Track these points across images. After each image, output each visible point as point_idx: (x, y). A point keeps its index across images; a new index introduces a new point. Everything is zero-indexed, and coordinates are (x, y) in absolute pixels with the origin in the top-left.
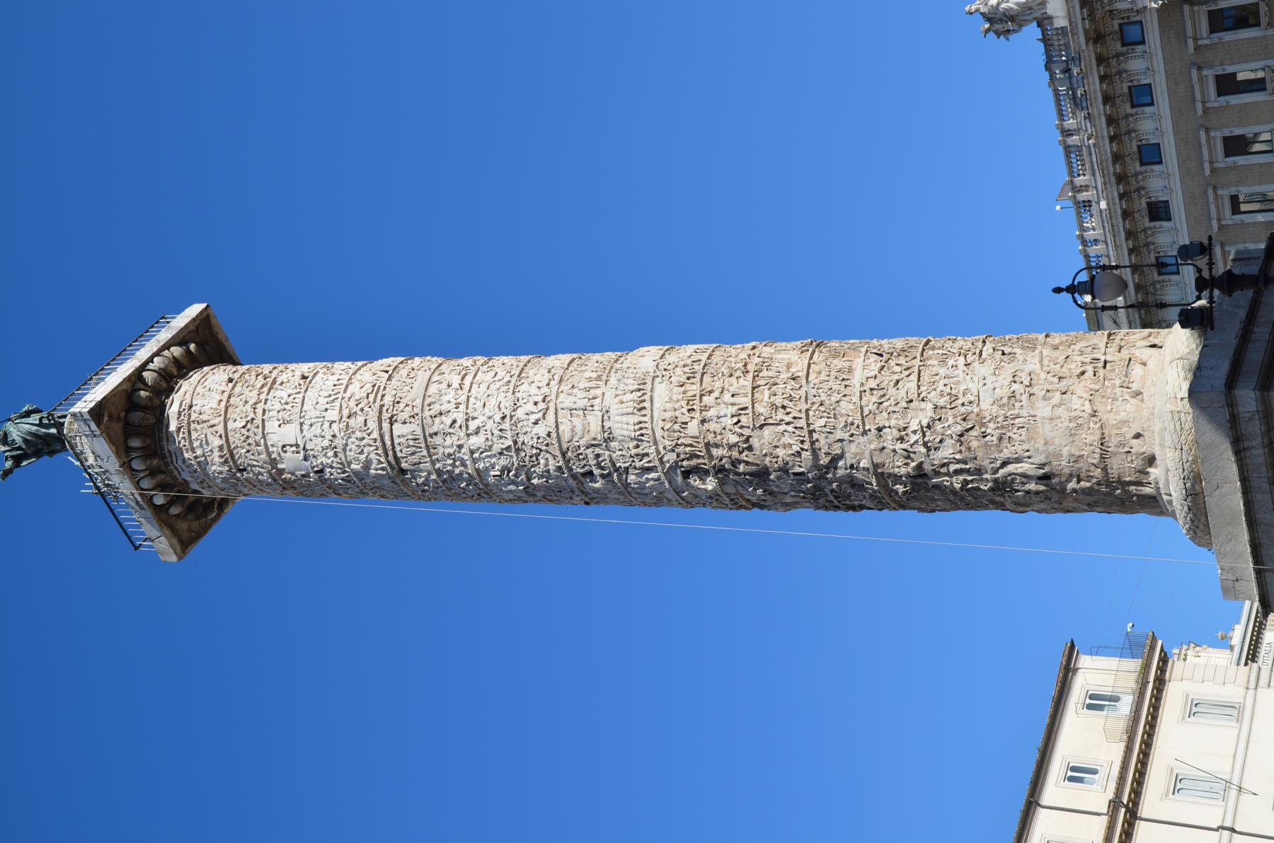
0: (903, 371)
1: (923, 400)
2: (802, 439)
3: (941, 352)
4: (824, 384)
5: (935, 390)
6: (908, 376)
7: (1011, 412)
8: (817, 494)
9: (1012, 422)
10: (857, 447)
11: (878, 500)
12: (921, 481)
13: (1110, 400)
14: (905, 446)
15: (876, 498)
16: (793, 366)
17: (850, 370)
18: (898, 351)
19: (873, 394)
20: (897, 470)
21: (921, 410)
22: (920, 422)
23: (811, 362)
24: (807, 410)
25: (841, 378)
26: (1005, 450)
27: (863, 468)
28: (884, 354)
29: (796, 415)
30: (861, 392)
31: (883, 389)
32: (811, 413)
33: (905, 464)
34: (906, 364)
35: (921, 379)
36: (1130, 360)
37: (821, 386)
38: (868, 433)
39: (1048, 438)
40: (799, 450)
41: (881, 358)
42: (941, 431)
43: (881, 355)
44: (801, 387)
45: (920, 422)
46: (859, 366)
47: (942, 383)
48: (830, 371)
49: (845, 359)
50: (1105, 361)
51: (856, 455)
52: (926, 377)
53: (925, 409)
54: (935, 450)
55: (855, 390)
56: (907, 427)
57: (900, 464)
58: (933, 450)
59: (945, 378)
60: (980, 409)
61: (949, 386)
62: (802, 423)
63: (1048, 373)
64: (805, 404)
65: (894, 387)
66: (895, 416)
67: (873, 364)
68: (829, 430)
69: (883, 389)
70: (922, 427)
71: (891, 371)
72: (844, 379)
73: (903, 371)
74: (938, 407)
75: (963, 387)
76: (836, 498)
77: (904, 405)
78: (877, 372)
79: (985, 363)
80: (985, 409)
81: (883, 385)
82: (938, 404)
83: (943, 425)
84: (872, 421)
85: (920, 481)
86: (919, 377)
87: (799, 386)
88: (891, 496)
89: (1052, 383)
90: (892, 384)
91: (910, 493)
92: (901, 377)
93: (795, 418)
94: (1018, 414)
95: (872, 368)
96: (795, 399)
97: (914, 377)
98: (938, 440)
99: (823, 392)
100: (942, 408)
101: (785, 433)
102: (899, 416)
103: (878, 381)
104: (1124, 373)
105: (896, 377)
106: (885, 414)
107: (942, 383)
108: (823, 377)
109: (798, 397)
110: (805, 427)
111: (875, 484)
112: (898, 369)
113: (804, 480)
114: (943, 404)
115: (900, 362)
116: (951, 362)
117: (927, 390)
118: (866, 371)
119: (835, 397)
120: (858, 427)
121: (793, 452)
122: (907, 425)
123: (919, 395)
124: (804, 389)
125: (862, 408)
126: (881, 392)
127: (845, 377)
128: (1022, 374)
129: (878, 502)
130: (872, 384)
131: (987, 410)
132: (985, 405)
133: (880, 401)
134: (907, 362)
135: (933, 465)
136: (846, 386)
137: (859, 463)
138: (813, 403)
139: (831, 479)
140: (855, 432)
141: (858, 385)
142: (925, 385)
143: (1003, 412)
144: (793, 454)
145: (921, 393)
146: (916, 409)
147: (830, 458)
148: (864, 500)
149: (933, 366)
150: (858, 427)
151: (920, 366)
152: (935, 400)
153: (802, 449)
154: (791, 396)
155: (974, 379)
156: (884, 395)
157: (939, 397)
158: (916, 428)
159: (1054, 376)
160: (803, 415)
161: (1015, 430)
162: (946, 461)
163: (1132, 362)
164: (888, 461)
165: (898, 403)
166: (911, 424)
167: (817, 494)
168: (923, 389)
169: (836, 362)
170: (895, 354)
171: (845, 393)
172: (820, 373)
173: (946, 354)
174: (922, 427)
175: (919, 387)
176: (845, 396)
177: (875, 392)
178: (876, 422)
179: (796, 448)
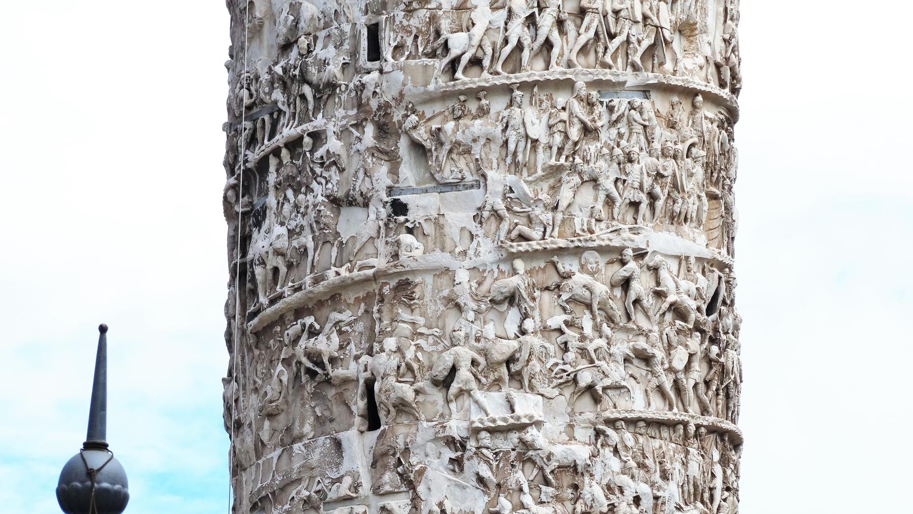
0: (672, 377)
1: (598, 433)
2: (486, 62)
3: (718, 483)
4: (642, 138)
5: (625, 470)
6: (660, 389)
8: (307, 90)
10: (463, 229)
11: (283, 270)
12: (354, 408)
14: (464, 373)
15: (290, 266)
16: (685, 43)
17: (676, 218)
18: (722, 360)
19: (613, 286)
20: (390, 343)
21: (571, 426)
22: (538, 424)
23: (700, 98)
24: (568, 85)
25: (657, 189)
27: (398, 243)
28: (714, 316)
29: (556, 51)
30: (621, 250)
31: (629, 318)
32: (561, 99)
33: (409, 368)
34: (692, 383)
35: (652, 431)
37: (638, 128)
38: (504, 267)
40: (454, 52)
41: (704, 307)
42: (512, 482)
43: (710, 310)
44: (635, 68)
45: (538, 424)
46: (689, 243)
47: (644, 489)
48: (675, 157)
49: (705, 199)
51: (438, 222)
52: (656, 443)
53: (572, 438)
54: (452, 461)
55: (627, 234)
56: (521, 382)
57: (410, 354)
58: (453, 455)
59: (656, 498)
62: (534, 71)
64: (590, 78)
65: (635, 350)
66: (552, 348)
67: (693, 287)
68: (512, 146)
69: (629, 318)
70: (522, 427)
71: (674, 339)
72: (653, 197)
73: (672, 377)
74: (578, 480)
76: (294, 145)
77: (585, 379)
78: (671, 298)
81: (640, 319)
82: (587, 479)
83: (526, 488)
84: (539, 279)
85: (360, 405)
86: (659, 424)
87: (637, 59)
88: (299, 312)
90: (642, 343)
91: (312, 374)
92: (659, 369)
93: (548, 45)
95: (684, 284)
96: (601, 50)
97: (657, 409)
98: (486, 472)
99: (620, 136)
100: (576, 487)
101: (503, 13)
102: (552, 361)
103: (649, 301)
105: (659, 354)
106: (557, 320)
107: (644, 489)
108: (661, 134)
109: (608, 59)
110: (523, 77)
111: (344, 272)
112: (679, 359)
113: (354, 54)
114: (586, 491)
115: (696, 365)
118: (674, 265)
119: (608, 173)
120: (522, 237)
121: (445, 34)
122: (526, 383)
124: (631, 79)
125: (578, 251)
126: (619, 313)
127: (659, 204)
129: (276, 270)
130: (641, 286)
133: (595, 307)
134: (695, 386)
135: (407, 450)
136: (635, 205)
137: (410, 231)
138: (591, 105)
139: (360, 139)
140: (505, 226)
141: (639, 241)
142: (637, 441)
144: (438, 34)
145: (616, 429)
146: (572, 414)
147: (428, 144)
148: (283, 231)
149: (685, 464)
150: (522, 237)
151: (685, 424)
152: (598, 470)
153: (453, 65)
154: (612, 36)
156: (610, 319)
157: (605, 482)
158: (519, 411)
160: (557, 72)
162: (421, 489)
164: (421, 321)
165: (592, 361)
166: (530, 396)
167: (307, 90)
168: (629, 437)
169: (699, 171)
170: (715, 349)
171: (619, 201)
172: (672, 125)
173: (712, 499)
174: (522, 427)
175: (632, 422)
176: (610, 201)
177: (618, 292)
178: (537, 294)
179: (458, 43)
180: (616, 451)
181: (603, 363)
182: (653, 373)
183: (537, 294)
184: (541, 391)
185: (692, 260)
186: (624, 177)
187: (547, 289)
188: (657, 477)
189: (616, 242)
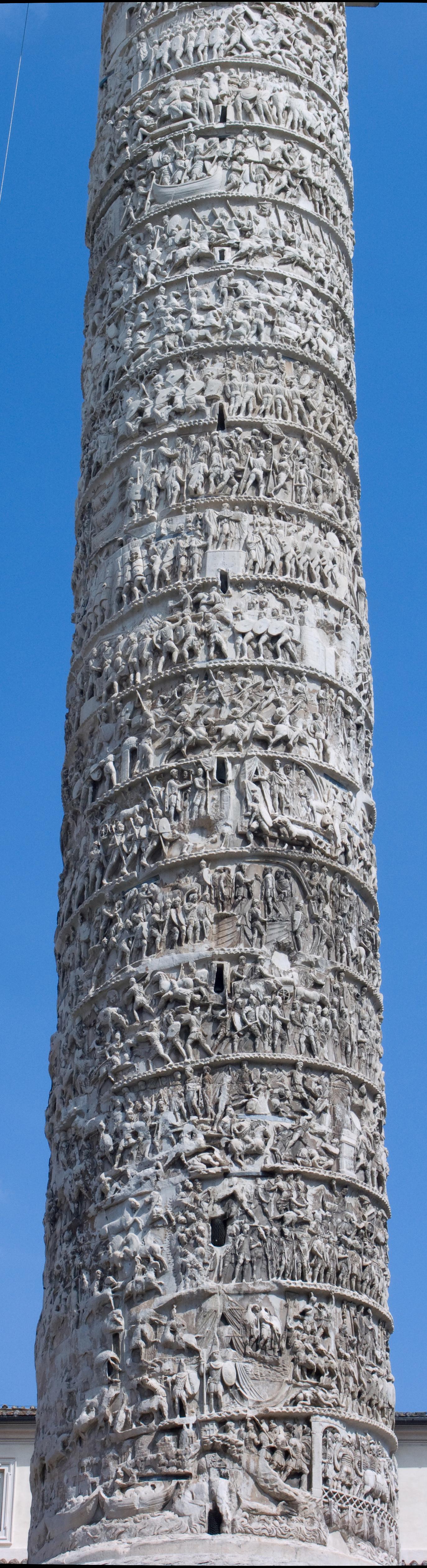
36: (187, 1476)
50: (180, 1427)
61: (132, 1141)
63: (154, 1325)
73: (169, 1045)
75: (131, 1169)
94: (83, 1291)
104: (150, 1471)
128: (151, 1274)
131: (94, 1230)
141: (140, 970)
143: (87, 1261)
151: (183, 1071)
154: (127, 855)
159: (144, 1337)
161: (64, 1295)
163: (174, 1482)
173: (216, 1109)
180: (123, 1109)
183: (86, 1032)
185: (192, 964)
187: (90, 1026)
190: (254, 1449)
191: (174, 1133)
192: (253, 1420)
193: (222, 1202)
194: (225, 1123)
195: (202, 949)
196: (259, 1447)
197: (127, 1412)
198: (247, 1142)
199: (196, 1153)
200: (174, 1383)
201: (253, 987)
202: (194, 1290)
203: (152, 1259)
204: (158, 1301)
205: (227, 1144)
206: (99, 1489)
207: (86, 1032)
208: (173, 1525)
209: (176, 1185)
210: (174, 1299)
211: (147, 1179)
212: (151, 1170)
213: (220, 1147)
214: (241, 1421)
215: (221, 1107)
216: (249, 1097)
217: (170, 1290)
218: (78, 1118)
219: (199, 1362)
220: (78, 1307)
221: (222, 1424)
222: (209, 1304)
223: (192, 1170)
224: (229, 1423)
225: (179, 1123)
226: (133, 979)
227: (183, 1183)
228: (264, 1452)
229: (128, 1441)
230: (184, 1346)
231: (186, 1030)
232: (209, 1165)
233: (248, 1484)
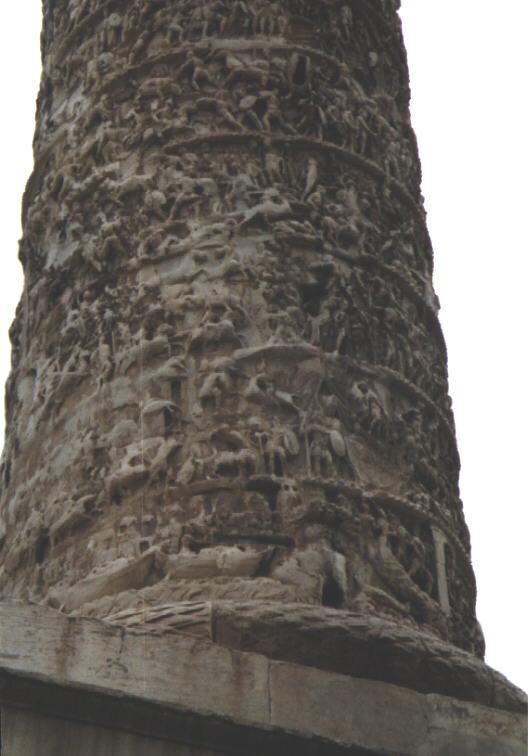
7: (124, 328)
9: (102, 338)
13: (148, 517)
26: (49, 360)
39: (66, 428)
45: (112, 175)
60: (135, 271)
73: (241, 116)
77: (148, 132)
79: (269, 253)
80: (137, 280)
83: (104, 220)
89: (199, 385)
104: (234, 532)
106: (132, 112)
116: (272, 191)
117: (188, 163)
122: (106, 158)
123: (174, 151)
132: (147, 278)
145: (180, 155)
146: (141, 161)
149: (262, 164)
151: (260, 141)
155: (218, 237)
161: (84, 353)
163: (270, 548)
168: (192, 157)
175: (194, 147)
180: (179, 167)
181: (165, 120)
182: (221, 115)
183: (115, 106)
184: (118, 157)
186: (187, 18)
188: (224, 171)
189: (177, 50)
190: (371, 533)
191: (252, 196)
192: (368, 500)
193: (317, 271)
194: (315, 197)
195: (279, 41)
196: (378, 533)
197: (196, 465)
198: (341, 223)
199: (284, 217)
200: (265, 440)
201: (339, 92)
202: (291, 345)
203: (228, 308)
204: (238, 353)
205: (319, 219)
206: (152, 549)
207: (115, 106)
208: (273, 592)
209: (258, 243)
210: (264, 351)
211: (216, 232)
212: (220, 226)
213: (309, 220)
214: (356, 498)
215: (310, 182)
216: (341, 187)
217: (255, 344)
218: (107, 180)
219: (298, 421)
220: (110, 359)
221: (332, 493)
222: (309, 366)
223: (278, 231)
224: (340, 496)
225: (257, 186)
226: (191, 52)
227: (266, 243)
228: (384, 540)
229: (200, 498)
230: (277, 403)
231: (261, 106)
232: (298, 229)
233: (366, 570)
